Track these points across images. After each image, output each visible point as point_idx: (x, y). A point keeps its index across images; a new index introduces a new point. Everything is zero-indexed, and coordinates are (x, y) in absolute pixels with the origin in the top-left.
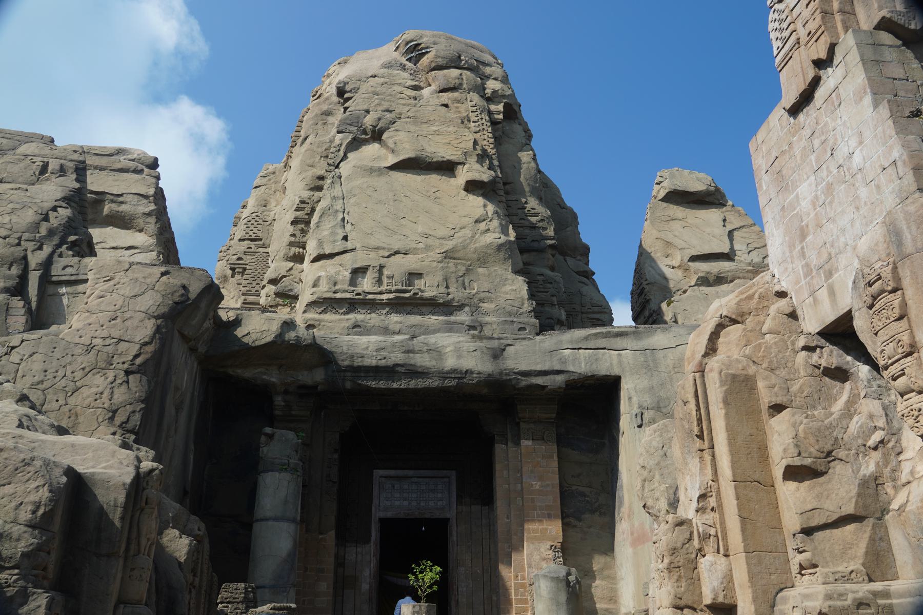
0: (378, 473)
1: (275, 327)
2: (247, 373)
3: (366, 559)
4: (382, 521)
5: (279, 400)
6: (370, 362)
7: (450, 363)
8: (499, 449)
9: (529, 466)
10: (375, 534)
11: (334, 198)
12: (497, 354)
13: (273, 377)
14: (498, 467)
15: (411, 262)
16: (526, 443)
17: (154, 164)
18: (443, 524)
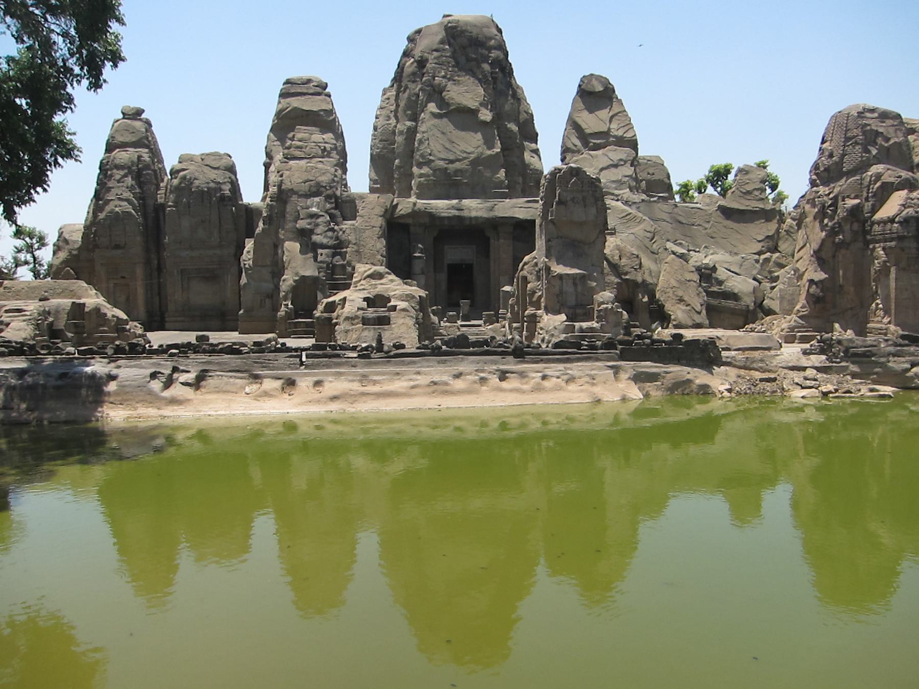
0: (446, 247)
1: (411, 205)
2: (402, 221)
3: (443, 277)
4: (449, 266)
5: (412, 229)
6: (446, 215)
7: (474, 214)
8: (492, 241)
9: (502, 247)
10: (446, 269)
11: (423, 132)
12: (492, 209)
13: (410, 221)
14: (491, 249)
15: (457, 165)
16: (502, 241)
17: (325, 86)
18: (470, 267)
